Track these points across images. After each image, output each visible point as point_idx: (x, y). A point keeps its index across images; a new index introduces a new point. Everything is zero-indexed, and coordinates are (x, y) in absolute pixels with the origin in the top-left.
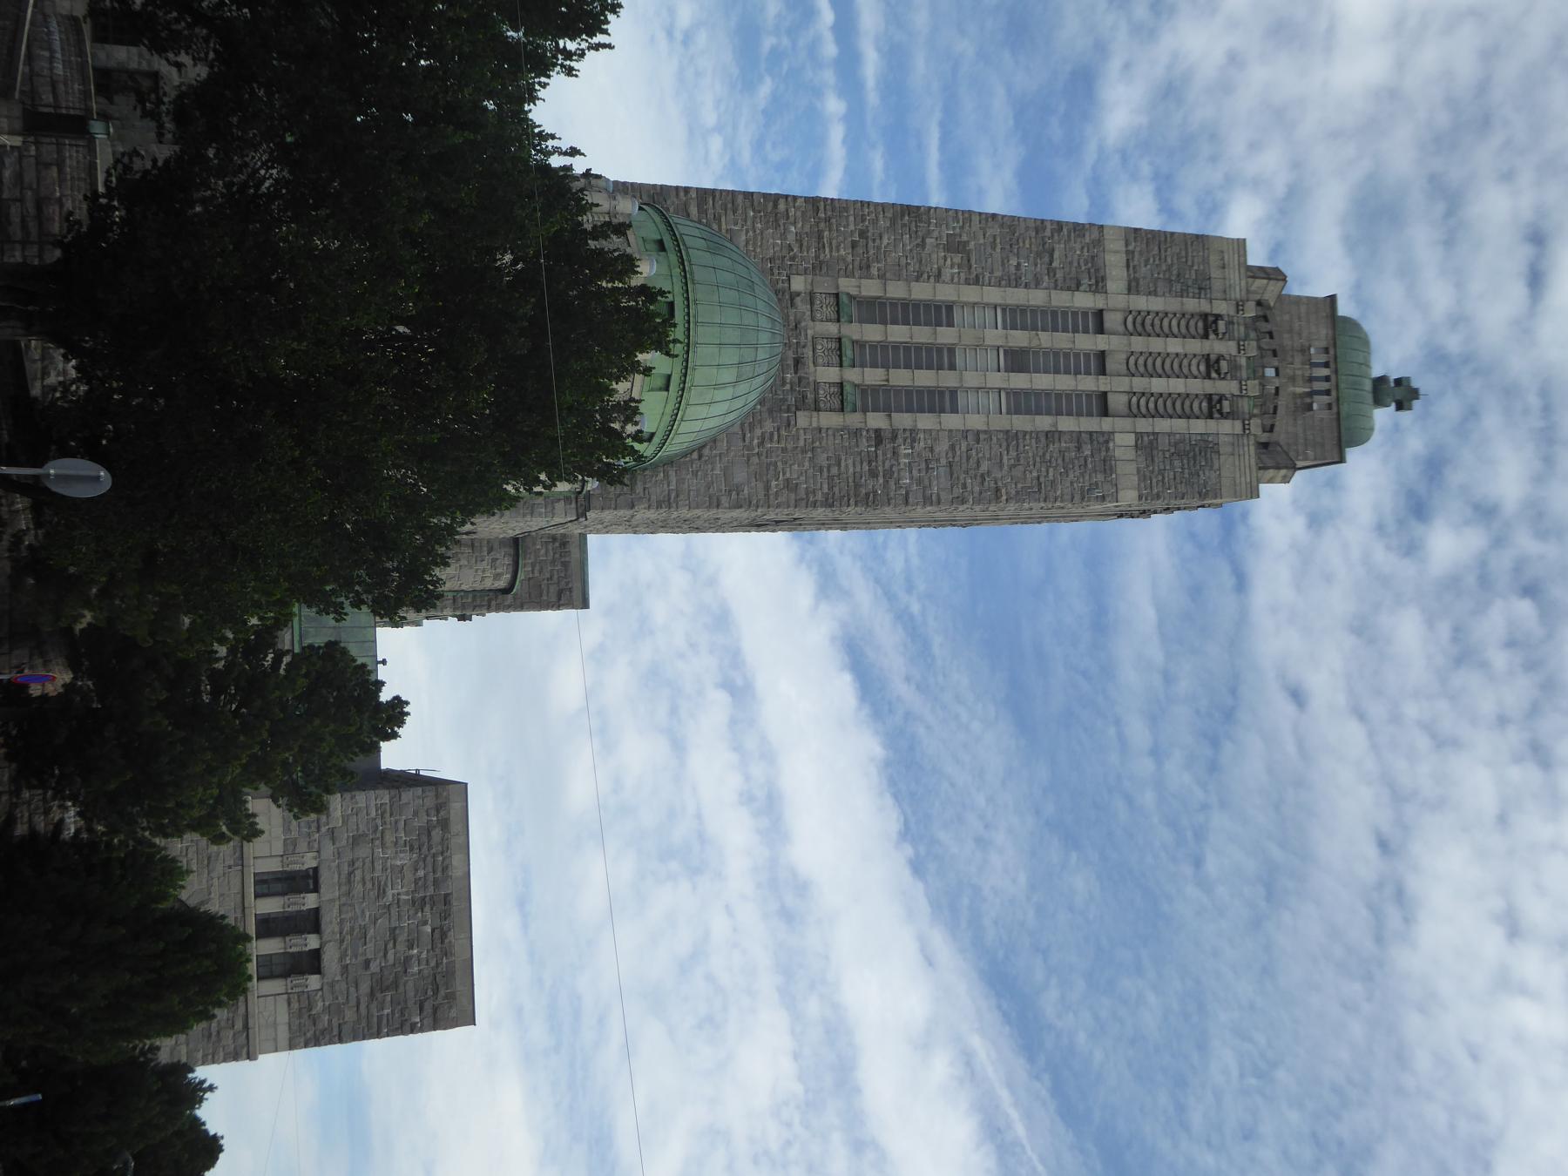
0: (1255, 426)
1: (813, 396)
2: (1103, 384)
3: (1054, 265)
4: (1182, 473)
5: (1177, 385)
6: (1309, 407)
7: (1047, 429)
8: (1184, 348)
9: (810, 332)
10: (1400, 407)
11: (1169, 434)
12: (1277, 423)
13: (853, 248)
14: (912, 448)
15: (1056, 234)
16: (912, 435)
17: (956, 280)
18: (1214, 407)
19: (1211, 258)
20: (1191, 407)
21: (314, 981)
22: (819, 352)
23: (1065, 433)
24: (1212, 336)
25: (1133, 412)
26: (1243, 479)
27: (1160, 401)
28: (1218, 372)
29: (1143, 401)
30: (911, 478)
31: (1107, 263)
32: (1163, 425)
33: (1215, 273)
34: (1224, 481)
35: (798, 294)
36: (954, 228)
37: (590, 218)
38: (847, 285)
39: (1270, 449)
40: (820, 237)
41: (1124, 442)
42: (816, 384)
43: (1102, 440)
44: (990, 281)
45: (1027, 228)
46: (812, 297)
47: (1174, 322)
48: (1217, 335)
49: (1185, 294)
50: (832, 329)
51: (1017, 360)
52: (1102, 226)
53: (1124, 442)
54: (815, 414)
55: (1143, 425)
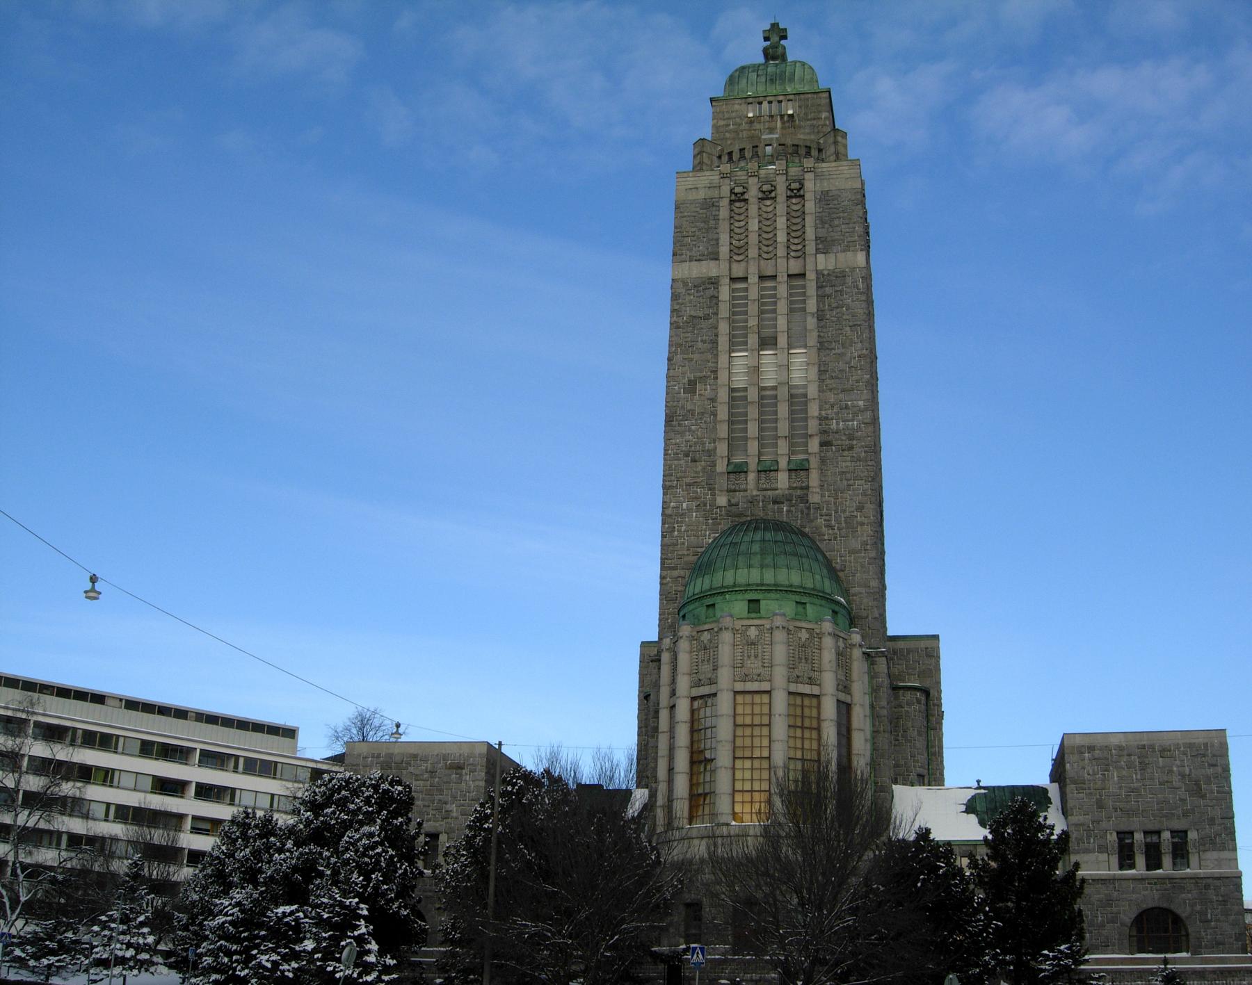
0: (808, 163)
1: (799, 491)
2: (782, 278)
3: (700, 315)
4: (844, 218)
5: (781, 222)
6: (791, 116)
7: (815, 320)
8: (755, 218)
9: (755, 493)
10: (784, 37)
11: (816, 228)
12: (805, 144)
13: (695, 461)
14: (832, 419)
15: (680, 314)
16: (821, 419)
17: (714, 387)
18: (796, 193)
19: (690, 198)
20: (796, 211)
21: (1192, 835)
22: (768, 487)
23: (818, 306)
24: (746, 196)
25: (802, 255)
26: (845, 172)
27: (793, 234)
28: (771, 192)
29: (794, 247)
30: (853, 420)
31: (698, 276)
32: (810, 233)
33: (701, 194)
34: (848, 186)
35: (729, 501)
36: (680, 388)
37: (695, 653)
38: (721, 467)
39: (822, 147)
40: (688, 485)
41: (824, 262)
42: (790, 488)
43: (824, 279)
44: (714, 362)
45: (677, 335)
46: (729, 491)
47: (737, 224)
48: (744, 193)
49: (716, 217)
50: (752, 476)
52: (673, 280)
53: (824, 262)
54: (811, 490)
55: (811, 248)
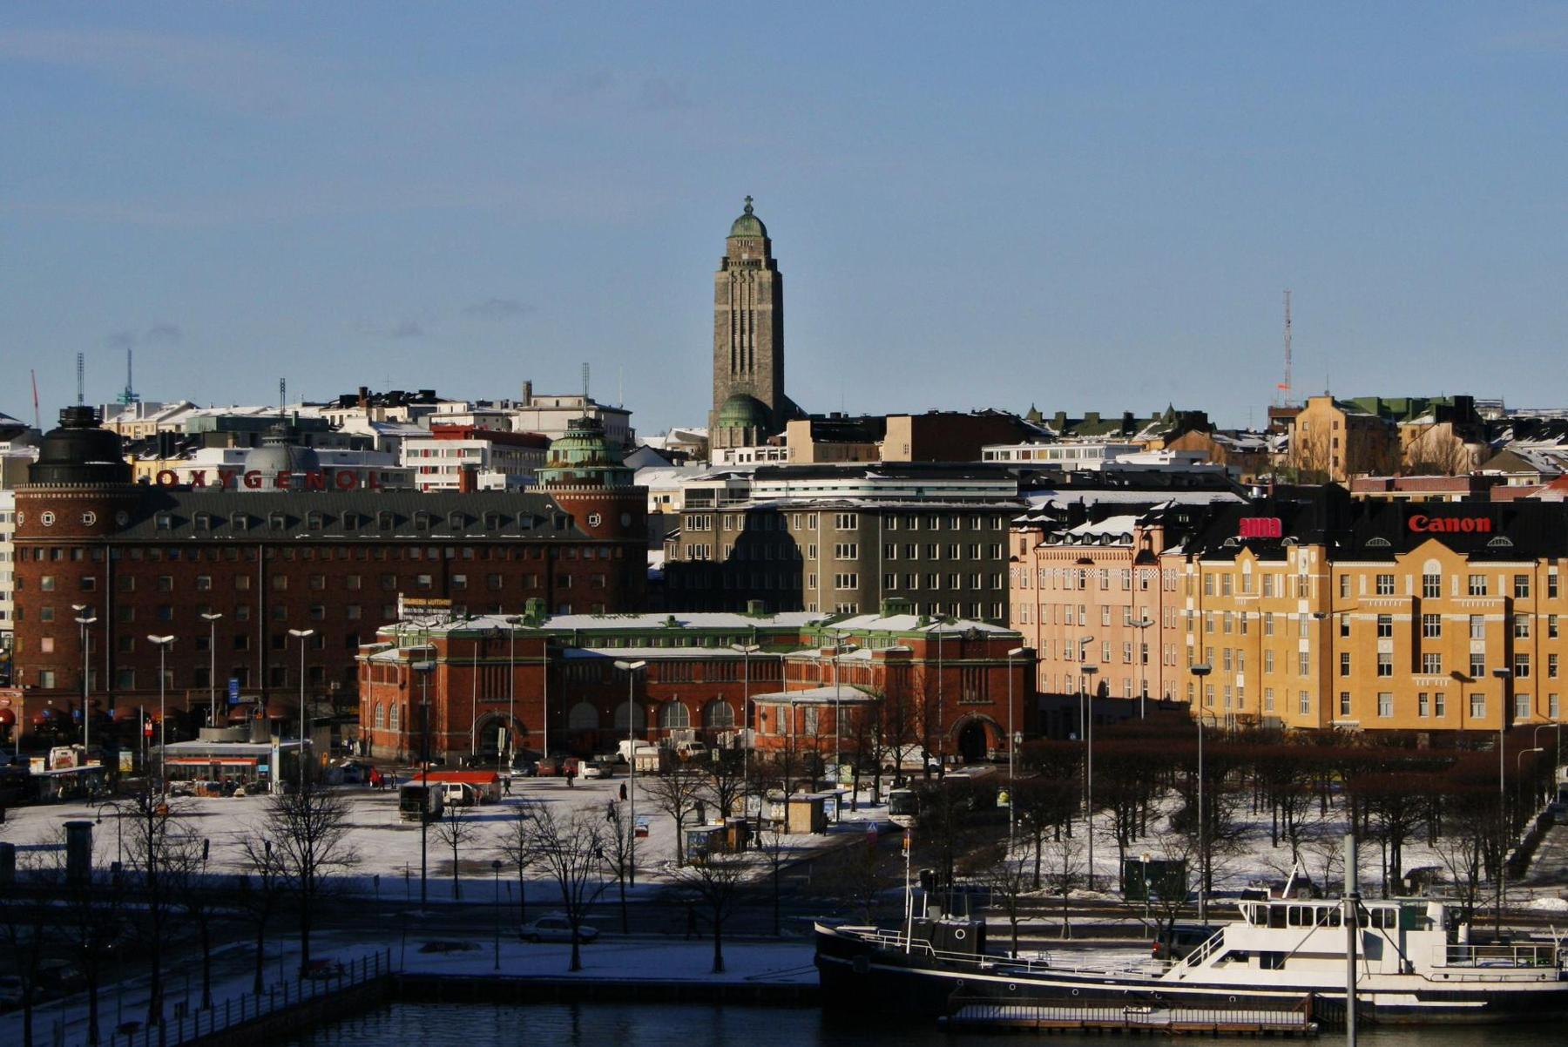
32: (756, 297)
33: (723, 280)
51: (742, 332)
